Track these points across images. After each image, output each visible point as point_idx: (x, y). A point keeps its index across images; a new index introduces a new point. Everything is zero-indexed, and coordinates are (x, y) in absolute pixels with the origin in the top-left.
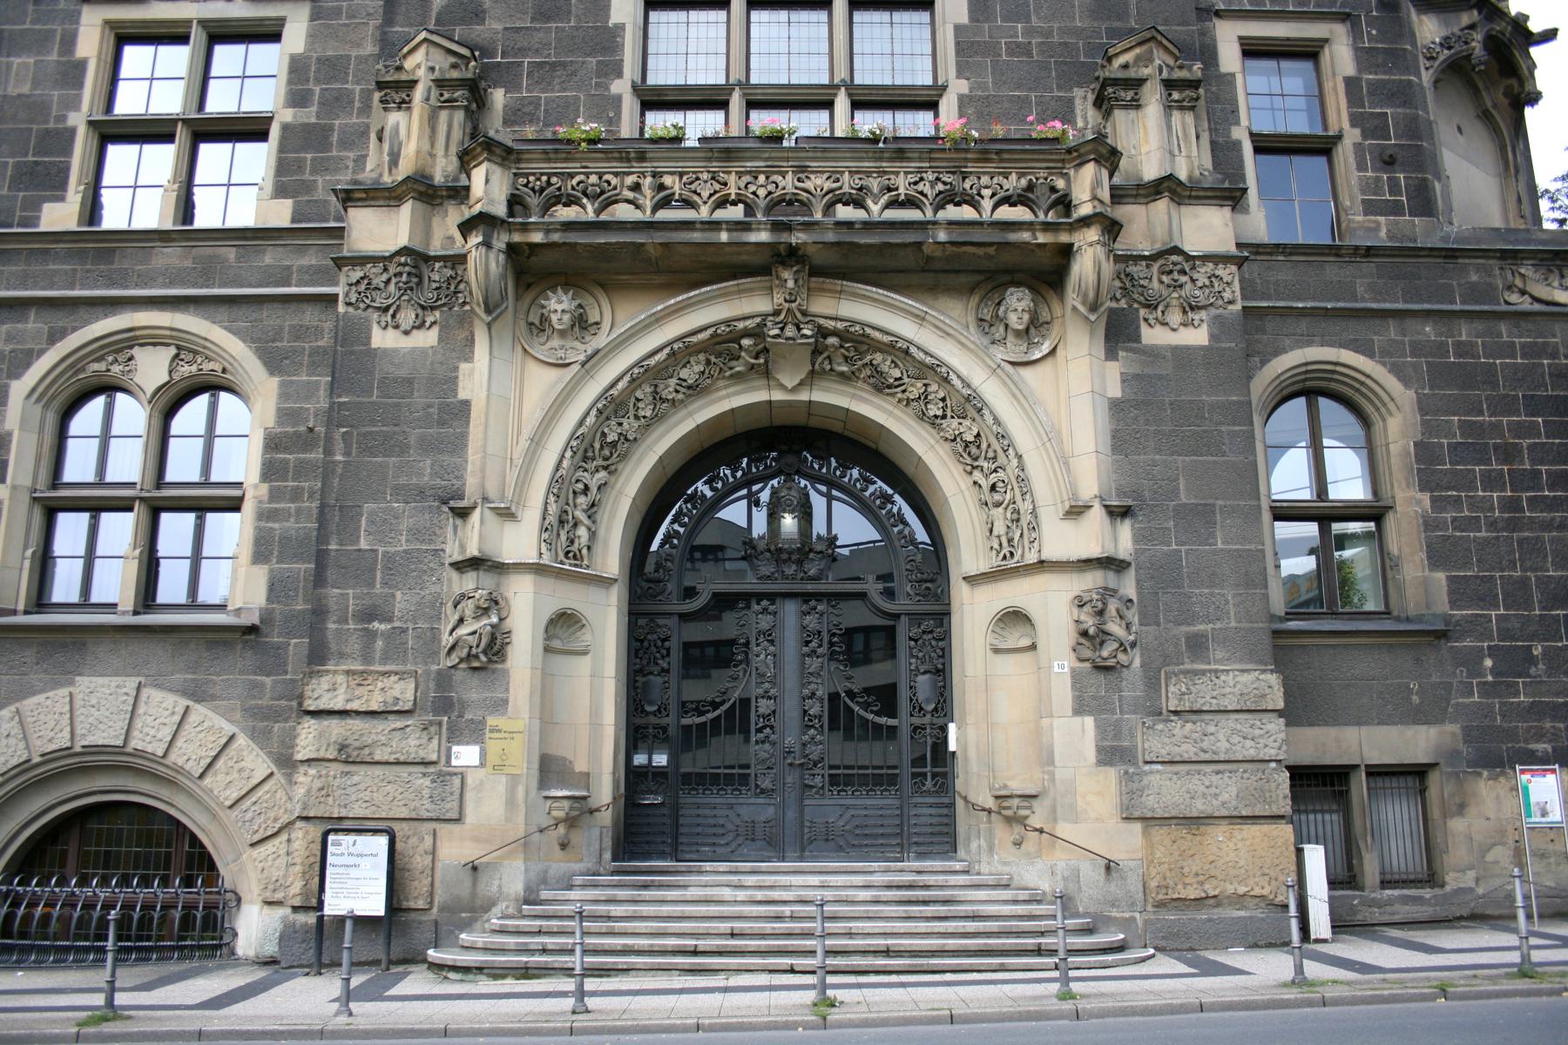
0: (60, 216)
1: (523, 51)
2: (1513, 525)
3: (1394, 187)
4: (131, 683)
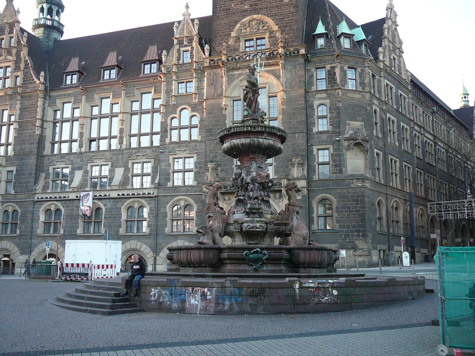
0: (170, 184)
1: (222, 162)
2: (349, 217)
3: (337, 169)
4: (183, 241)
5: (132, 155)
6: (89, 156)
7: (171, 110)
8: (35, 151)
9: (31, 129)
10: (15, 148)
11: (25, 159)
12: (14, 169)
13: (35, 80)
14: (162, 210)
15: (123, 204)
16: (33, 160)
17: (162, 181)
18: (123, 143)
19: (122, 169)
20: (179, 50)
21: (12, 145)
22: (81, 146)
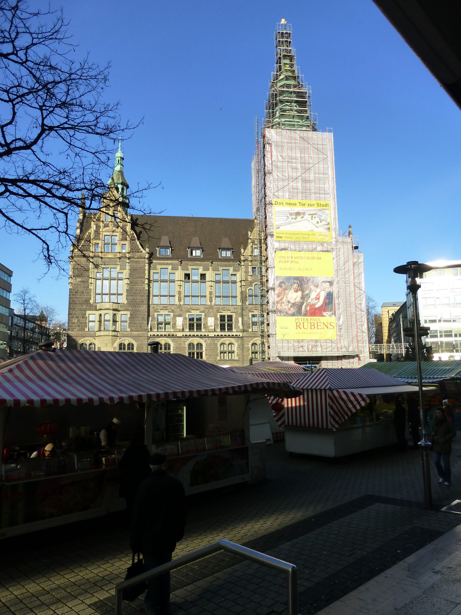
5: (220, 310)
6: (187, 308)
7: (248, 284)
8: (146, 302)
9: (141, 286)
10: (128, 298)
11: (138, 307)
12: (128, 313)
13: (142, 249)
14: (246, 346)
15: (219, 341)
16: (145, 308)
17: (245, 328)
18: (212, 301)
19: (213, 319)
20: (252, 246)
21: (125, 294)
22: (180, 300)
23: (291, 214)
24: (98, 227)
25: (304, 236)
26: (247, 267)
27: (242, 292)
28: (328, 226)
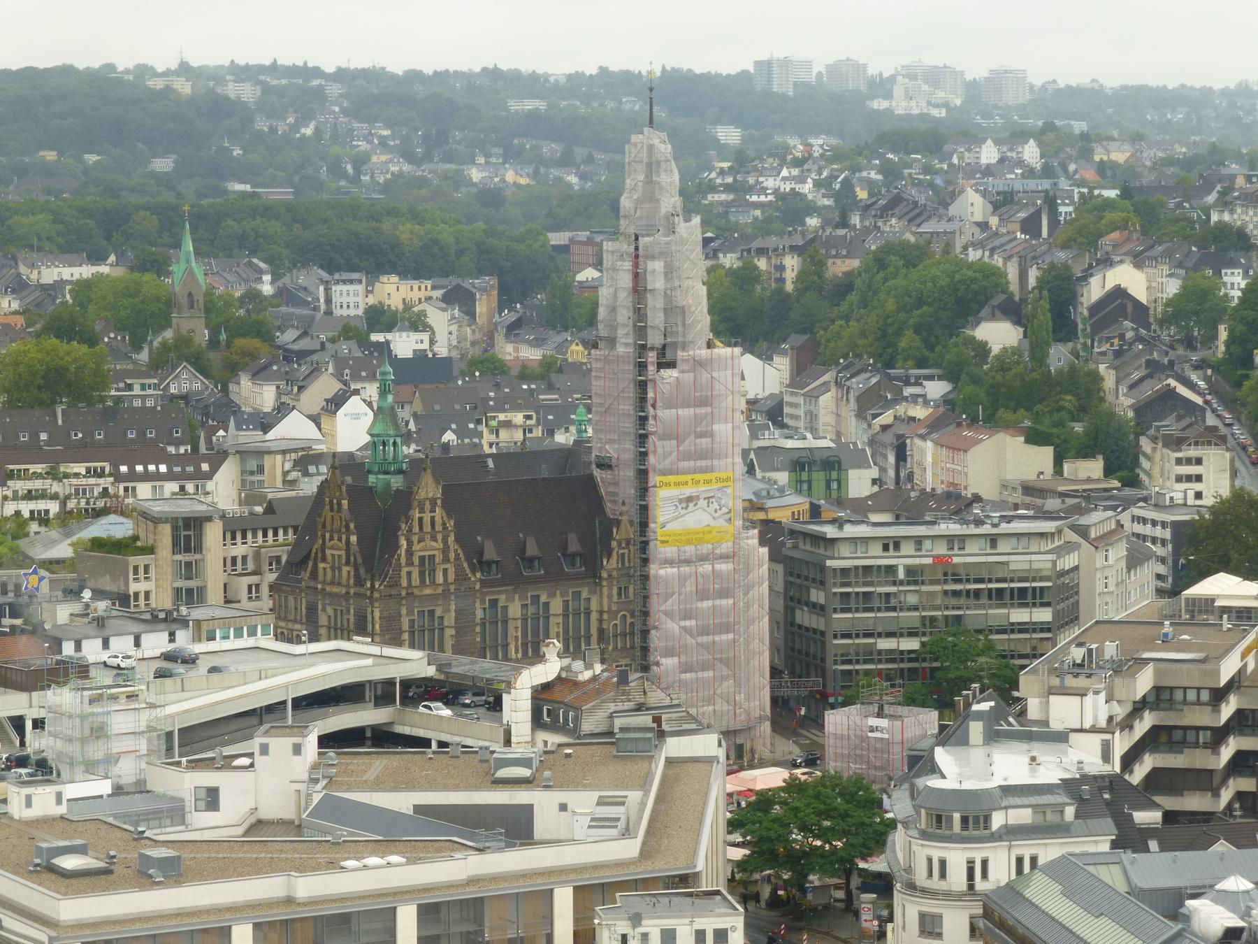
23: (681, 501)
24: (410, 543)
25: (697, 536)
26: (610, 589)
27: (601, 631)
28: (727, 516)
